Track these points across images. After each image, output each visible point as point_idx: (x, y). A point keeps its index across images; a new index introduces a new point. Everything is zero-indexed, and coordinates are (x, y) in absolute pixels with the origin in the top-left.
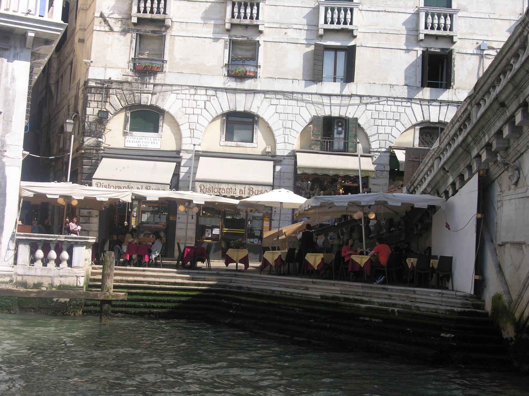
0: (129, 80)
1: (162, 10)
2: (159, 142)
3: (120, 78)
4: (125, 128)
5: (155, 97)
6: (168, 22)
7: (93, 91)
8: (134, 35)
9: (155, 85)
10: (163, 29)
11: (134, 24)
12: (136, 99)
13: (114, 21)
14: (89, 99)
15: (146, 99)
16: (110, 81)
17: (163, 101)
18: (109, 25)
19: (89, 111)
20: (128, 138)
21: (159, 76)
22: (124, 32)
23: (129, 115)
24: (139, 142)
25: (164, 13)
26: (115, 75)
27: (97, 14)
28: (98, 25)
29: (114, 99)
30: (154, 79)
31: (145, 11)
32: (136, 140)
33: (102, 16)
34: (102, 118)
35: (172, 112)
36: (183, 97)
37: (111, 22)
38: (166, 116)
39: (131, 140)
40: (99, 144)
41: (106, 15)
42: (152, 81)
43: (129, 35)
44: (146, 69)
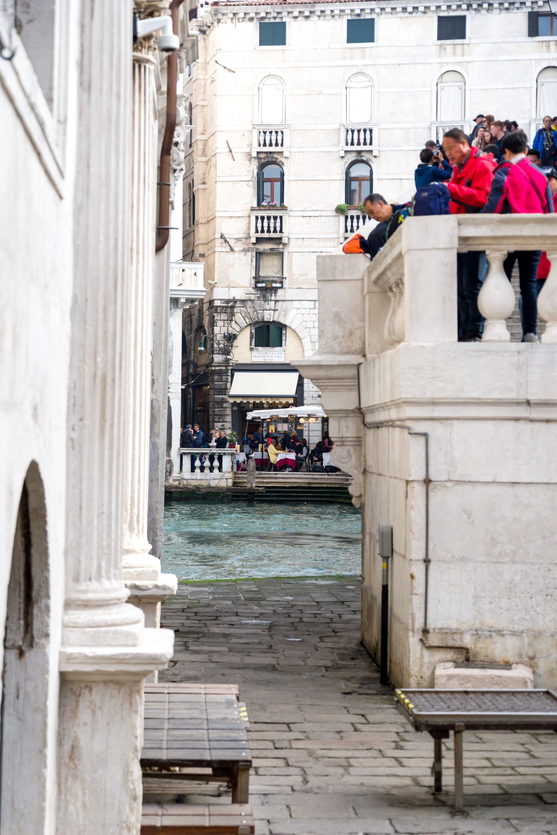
0: (252, 298)
1: (278, 229)
2: (283, 356)
3: (244, 297)
4: (251, 345)
5: (277, 312)
6: (285, 240)
7: (218, 311)
8: (254, 254)
9: (276, 301)
10: (281, 246)
11: (254, 244)
12: (260, 316)
13: (234, 241)
14: (216, 318)
15: (268, 316)
16: (235, 301)
17: (284, 316)
18: (229, 245)
19: (216, 330)
20: (255, 353)
21: (280, 292)
22: (245, 251)
23: (253, 331)
24: (265, 356)
25: (281, 231)
26: (239, 294)
27: (218, 236)
28: (219, 246)
29: (238, 317)
30: (275, 296)
31: (262, 231)
32: (261, 355)
33: (222, 237)
34: (231, 338)
35: (293, 326)
36: (304, 311)
37: (232, 243)
38: (288, 330)
39: (257, 355)
40: (227, 361)
41: (226, 236)
42: (273, 298)
43: (249, 254)
44: (266, 288)
